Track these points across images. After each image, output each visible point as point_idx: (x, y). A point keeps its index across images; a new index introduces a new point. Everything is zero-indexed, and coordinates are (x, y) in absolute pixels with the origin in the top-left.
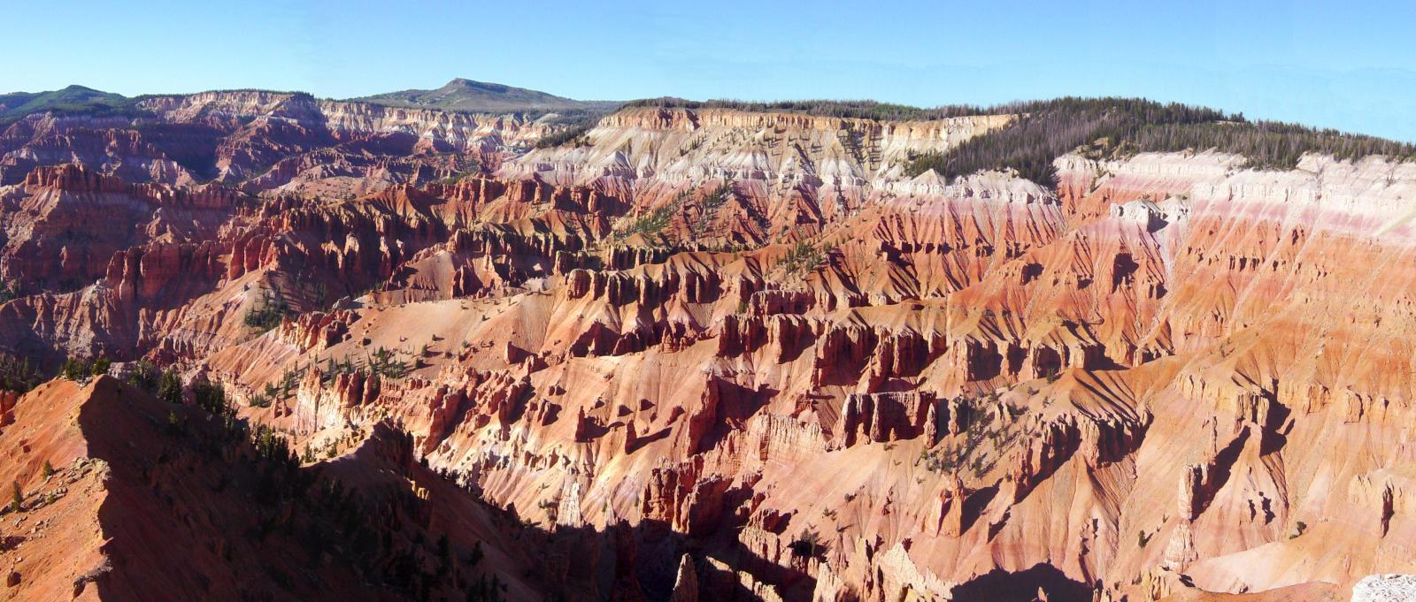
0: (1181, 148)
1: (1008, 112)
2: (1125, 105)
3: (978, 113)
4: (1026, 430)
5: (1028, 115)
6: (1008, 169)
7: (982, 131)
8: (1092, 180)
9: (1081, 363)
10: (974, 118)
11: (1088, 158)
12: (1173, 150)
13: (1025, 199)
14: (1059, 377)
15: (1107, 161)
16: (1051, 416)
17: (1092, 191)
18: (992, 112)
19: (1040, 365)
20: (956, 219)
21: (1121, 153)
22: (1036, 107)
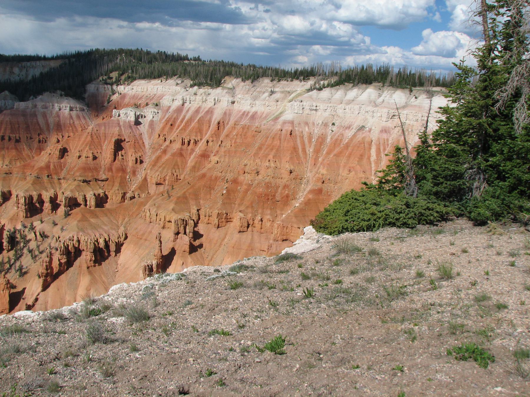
0: (159, 76)
2: (129, 53)
4: (50, 247)
5: (74, 60)
7: (46, 70)
9: (93, 203)
10: (43, 62)
11: (107, 84)
12: (155, 78)
13: (68, 109)
14: (70, 215)
15: (118, 85)
16: (65, 236)
18: (53, 58)
19: (69, 206)
21: (125, 80)
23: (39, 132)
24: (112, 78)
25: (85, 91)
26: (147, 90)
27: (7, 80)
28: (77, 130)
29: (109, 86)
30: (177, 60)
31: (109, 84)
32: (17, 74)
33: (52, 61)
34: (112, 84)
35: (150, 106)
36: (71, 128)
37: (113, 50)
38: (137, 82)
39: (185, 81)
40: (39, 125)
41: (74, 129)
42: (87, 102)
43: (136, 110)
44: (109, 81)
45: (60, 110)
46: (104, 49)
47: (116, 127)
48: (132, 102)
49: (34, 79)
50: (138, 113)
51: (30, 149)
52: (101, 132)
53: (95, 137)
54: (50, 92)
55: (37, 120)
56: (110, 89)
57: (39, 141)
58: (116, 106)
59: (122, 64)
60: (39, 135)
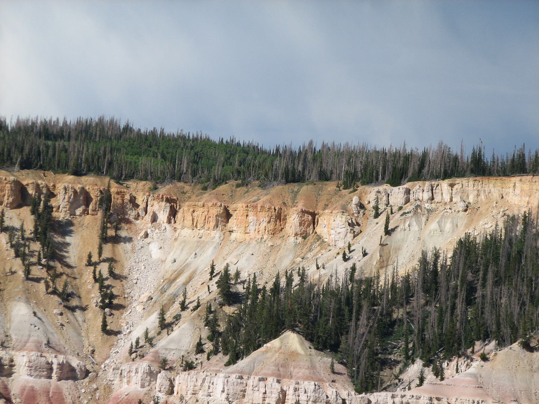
3: (479, 168)
10: (469, 187)
27: (290, 280)
32: (339, 246)
33: (516, 180)
49: (431, 275)
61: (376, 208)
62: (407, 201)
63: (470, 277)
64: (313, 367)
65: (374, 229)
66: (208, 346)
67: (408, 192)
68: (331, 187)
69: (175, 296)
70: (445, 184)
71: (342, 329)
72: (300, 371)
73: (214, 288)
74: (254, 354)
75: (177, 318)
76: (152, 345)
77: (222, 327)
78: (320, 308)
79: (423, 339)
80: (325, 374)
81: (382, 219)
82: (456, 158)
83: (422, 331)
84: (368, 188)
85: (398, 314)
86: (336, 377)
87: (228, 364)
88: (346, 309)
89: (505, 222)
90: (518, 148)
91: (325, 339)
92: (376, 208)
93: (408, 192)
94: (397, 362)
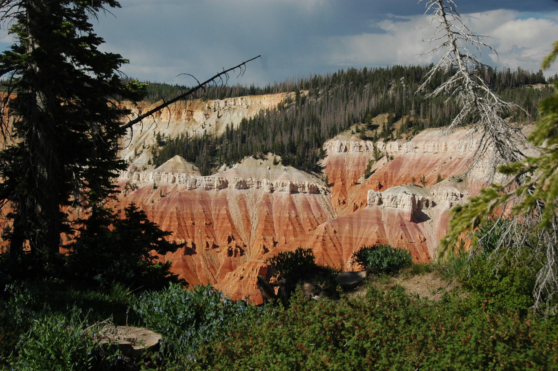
1: (285, 91)
3: (253, 92)
5: (306, 93)
6: (270, 154)
7: (252, 114)
8: (367, 164)
10: (248, 99)
11: (365, 139)
13: (287, 189)
15: (386, 141)
17: (367, 177)
20: (208, 217)
21: (402, 130)
22: (315, 84)
23: (230, 234)
24: (376, 127)
25: (323, 154)
26: (446, 149)
27: (182, 136)
28: (302, 231)
29: (369, 143)
30: (517, 85)
31: (371, 139)
33: (265, 96)
34: (374, 139)
35: (446, 180)
36: (291, 228)
37: (381, 70)
38: (425, 134)
39: (525, 127)
40: (231, 220)
41: (298, 229)
42: (324, 175)
43: (415, 190)
44: (369, 133)
45: (272, 191)
46: (365, 69)
47: (372, 224)
48: (414, 174)
49: (230, 133)
50: (419, 197)
51: (212, 267)
52: (344, 235)
53: (330, 245)
54: (255, 157)
55: (228, 211)
56: (371, 149)
57: (230, 253)
58: (382, 183)
59: (398, 98)
60: (230, 240)
61: (215, 108)
62: (226, 105)
63: (244, 132)
64: (186, 168)
65: (214, 116)
66: (152, 162)
67: (226, 102)
68: (198, 101)
69: (141, 143)
70: (239, 99)
71: (197, 154)
72: (181, 170)
73: (155, 140)
74: (164, 164)
75: (142, 152)
76: (132, 162)
77: (158, 154)
78: (188, 146)
79: (226, 156)
80: (190, 170)
81: (217, 112)
82: (244, 89)
83: (226, 153)
84: (211, 101)
85: (218, 147)
86: (194, 172)
87: (155, 168)
88: (198, 146)
89: (260, 112)
90: (268, 84)
91: (190, 158)
92: (215, 108)
93: (226, 102)
94: (217, 165)
